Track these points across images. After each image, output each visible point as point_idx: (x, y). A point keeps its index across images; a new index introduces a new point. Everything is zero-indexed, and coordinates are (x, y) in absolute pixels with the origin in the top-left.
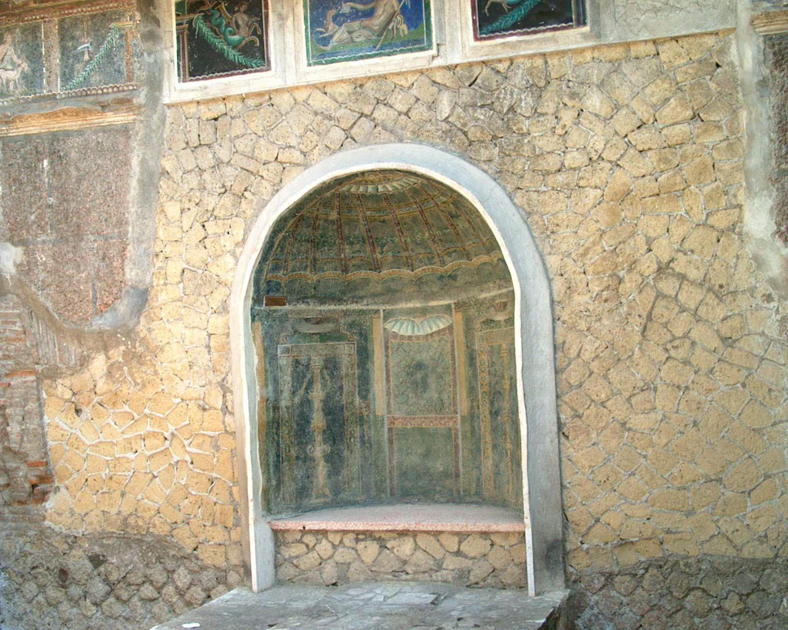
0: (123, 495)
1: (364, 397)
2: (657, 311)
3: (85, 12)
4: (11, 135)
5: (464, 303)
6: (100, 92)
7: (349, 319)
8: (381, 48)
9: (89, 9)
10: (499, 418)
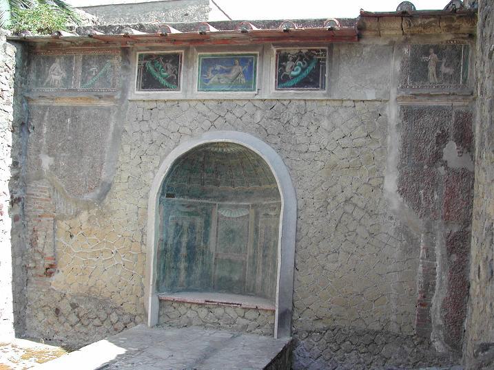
0: (90, 277)
2: (343, 219)
7: (202, 206)
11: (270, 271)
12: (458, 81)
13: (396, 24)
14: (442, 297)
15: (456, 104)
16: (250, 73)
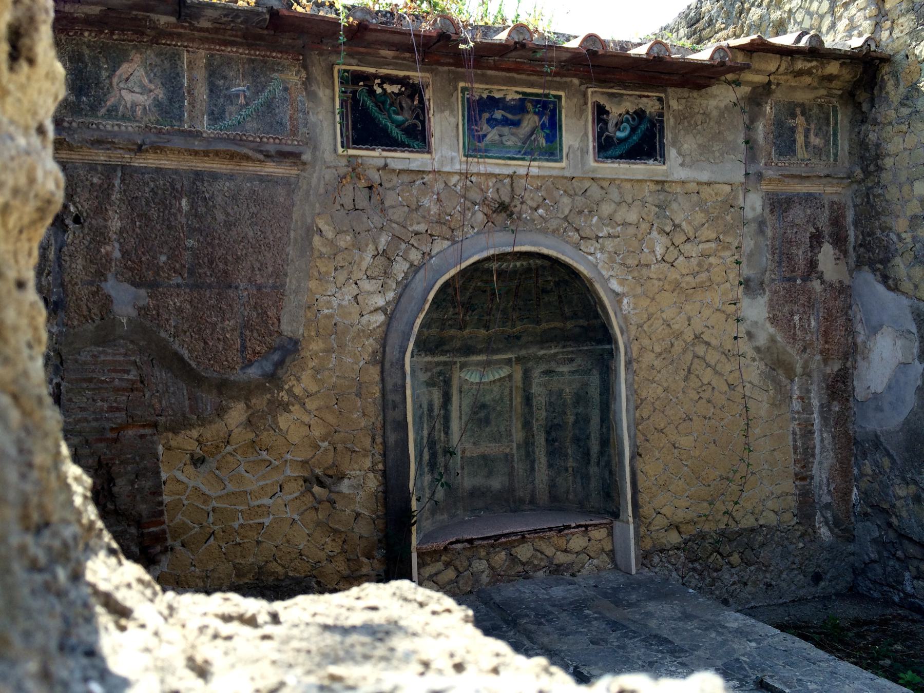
1: (446, 433)
2: (693, 367)
3: (241, 54)
4: (136, 165)
5: (524, 357)
6: (258, 140)
7: (439, 368)
8: (525, 154)
9: (247, 52)
10: (556, 444)
11: (571, 463)
12: (828, 157)
13: (772, 64)
14: (826, 464)
15: (829, 190)
16: (553, 128)
